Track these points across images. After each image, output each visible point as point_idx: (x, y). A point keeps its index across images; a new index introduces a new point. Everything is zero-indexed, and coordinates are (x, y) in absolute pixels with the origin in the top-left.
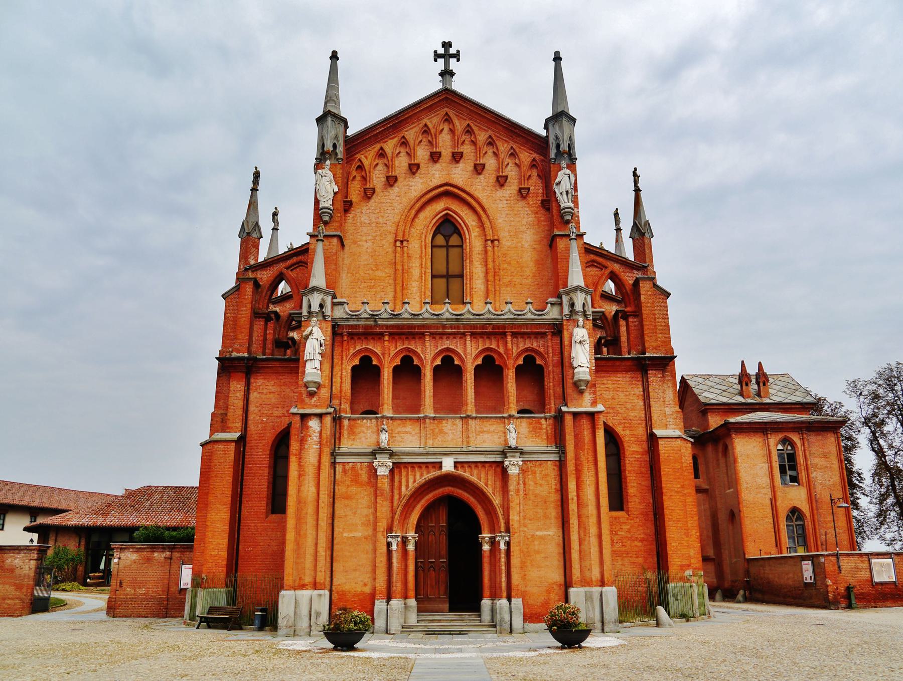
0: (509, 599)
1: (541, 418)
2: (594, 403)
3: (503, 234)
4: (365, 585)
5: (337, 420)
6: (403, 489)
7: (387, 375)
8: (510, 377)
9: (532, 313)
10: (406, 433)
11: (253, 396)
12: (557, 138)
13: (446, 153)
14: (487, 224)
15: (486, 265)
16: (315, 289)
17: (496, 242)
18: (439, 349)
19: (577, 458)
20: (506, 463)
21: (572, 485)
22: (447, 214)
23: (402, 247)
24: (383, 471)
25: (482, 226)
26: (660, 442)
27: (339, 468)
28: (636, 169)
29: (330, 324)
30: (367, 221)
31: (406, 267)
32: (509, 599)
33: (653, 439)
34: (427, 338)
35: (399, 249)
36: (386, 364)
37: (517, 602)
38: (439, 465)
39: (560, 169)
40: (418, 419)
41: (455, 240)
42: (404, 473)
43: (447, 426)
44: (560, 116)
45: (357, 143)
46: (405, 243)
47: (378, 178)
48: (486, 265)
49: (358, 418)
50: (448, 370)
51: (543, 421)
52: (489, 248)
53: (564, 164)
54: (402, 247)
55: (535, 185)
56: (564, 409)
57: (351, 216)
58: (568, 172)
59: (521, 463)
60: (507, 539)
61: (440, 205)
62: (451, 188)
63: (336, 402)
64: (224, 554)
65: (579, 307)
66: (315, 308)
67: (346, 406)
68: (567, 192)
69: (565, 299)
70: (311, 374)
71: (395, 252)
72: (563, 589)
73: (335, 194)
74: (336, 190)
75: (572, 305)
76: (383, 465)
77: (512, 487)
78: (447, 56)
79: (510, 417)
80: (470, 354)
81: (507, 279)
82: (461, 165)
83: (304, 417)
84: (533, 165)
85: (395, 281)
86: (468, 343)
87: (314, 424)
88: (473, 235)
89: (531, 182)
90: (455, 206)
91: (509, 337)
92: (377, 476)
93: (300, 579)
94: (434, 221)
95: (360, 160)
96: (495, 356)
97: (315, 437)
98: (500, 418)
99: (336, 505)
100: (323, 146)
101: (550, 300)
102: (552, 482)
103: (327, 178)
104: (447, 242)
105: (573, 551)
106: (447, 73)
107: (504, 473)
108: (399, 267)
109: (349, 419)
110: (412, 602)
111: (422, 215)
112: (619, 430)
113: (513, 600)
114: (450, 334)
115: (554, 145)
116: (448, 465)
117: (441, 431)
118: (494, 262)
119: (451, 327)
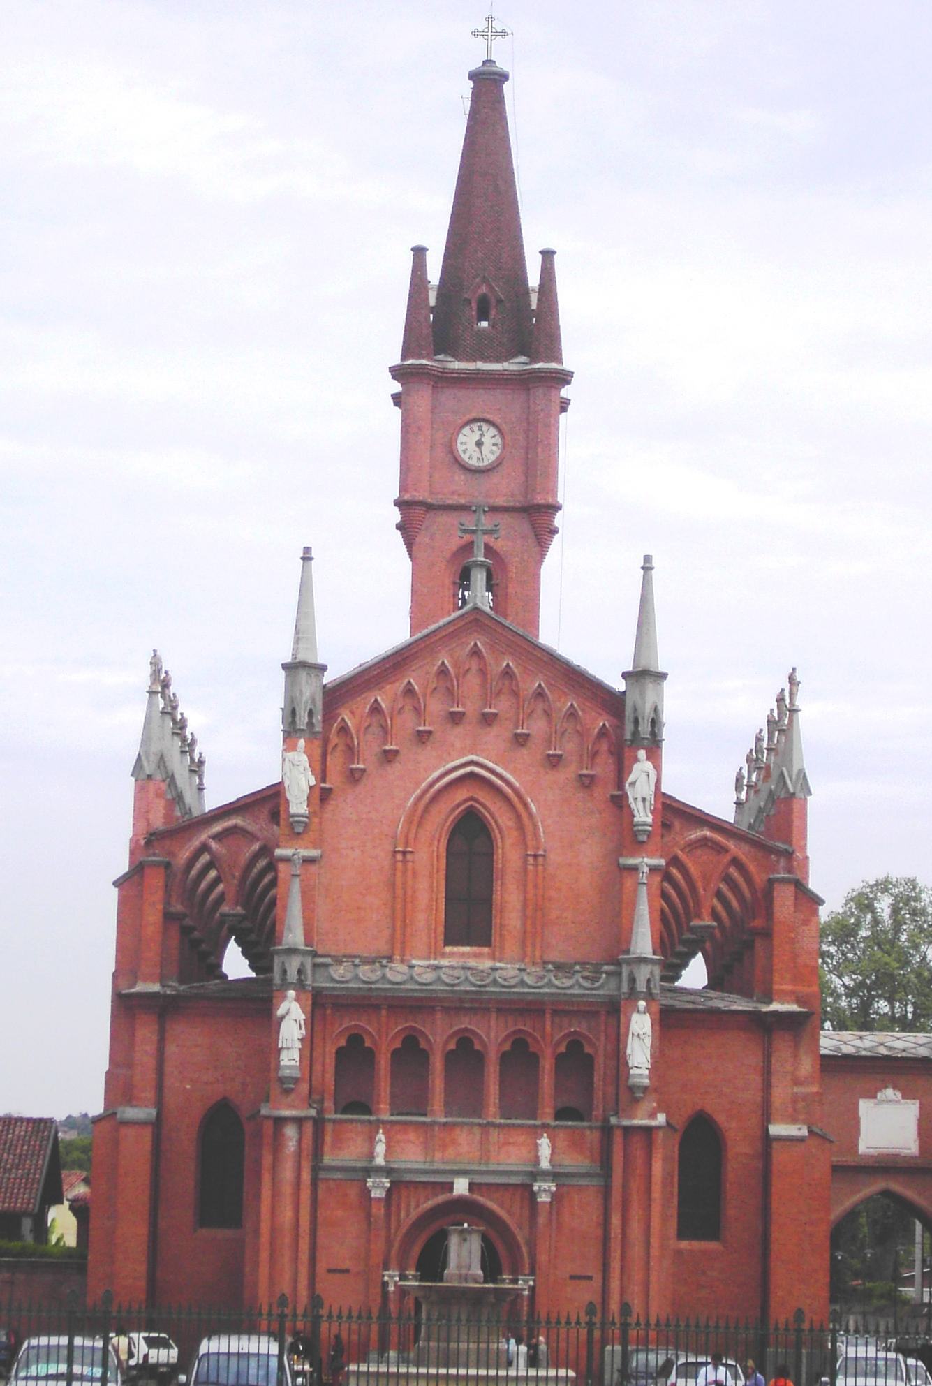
1: (584, 1128)
2: (653, 1116)
5: (319, 1123)
6: (403, 1214)
7: (383, 1063)
8: (547, 1064)
9: (581, 986)
10: (409, 1141)
11: (171, 1049)
12: (635, 710)
13: (470, 706)
15: (525, 892)
16: (292, 951)
17: (540, 859)
18: (456, 1028)
19: (625, 1186)
20: (536, 1188)
21: (616, 1220)
22: (471, 806)
23: (405, 862)
24: (377, 1193)
25: (521, 827)
26: (775, 1145)
27: (321, 1186)
28: (794, 669)
29: (310, 995)
30: (354, 817)
31: (410, 892)
33: (767, 1140)
34: (439, 1015)
35: (400, 865)
36: (384, 1048)
38: (450, 1187)
39: (636, 760)
40: (424, 1123)
42: (404, 1193)
43: (462, 1136)
45: (337, 695)
46: (409, 857)
47: (369, 747)
48: (525, 892)
49: (346, 1121)
50: (466, 1054)
51: (588, 1132)
52: (530, 867)
53: (642, 754)
54: (405, 862)
55: (603, 768)
56: (613, 1120)
57: (330, 808)
58: (648, 766)
59: (554, 1189)
61: (461, 795)
63: (316, 1097)
64: (142, 1284)
65: (641, 986)
66: (292, 976)
67: (329, 1104)
68: (644, 800)
69: (625, 971)
70: (289, 1067)
71: (394, 868)
73: (311, 788)
74: (313, 782)
75: (633, 980)
76: (378, 1188)
77: (542, 1220)
79: (545, 1127)
80: (493, 1035)
81: (553, 915)
82: (495, 730)
83: (280, 1122)
84: (603, 732)
86: (493, 1022)
87: (290, 1131)
88: (508, 842)
89: (598, 760)
90: (483, 796)
91: (548, 1016)
92: (370, 1199)
94: (451, 818)
95: (343, 719)
96: (529, 1040)
97: (291, 1146)
98: (530, 1126)
99: (320, 1233)
100: (293, 712)
101: (606, 968)
102: (595, 1215)
103: (301, 769)
105: (612, 1302)
107: (533, 1195)
108: (399, 892)
109: (334, 1121)
111: (434, 810)
112: (721, 1119)
114: (471, 1009)
115: (631, 719)
116: (461, 1186)
117: (454, 1142)
118: (536, 886)
119: (472, 1001)
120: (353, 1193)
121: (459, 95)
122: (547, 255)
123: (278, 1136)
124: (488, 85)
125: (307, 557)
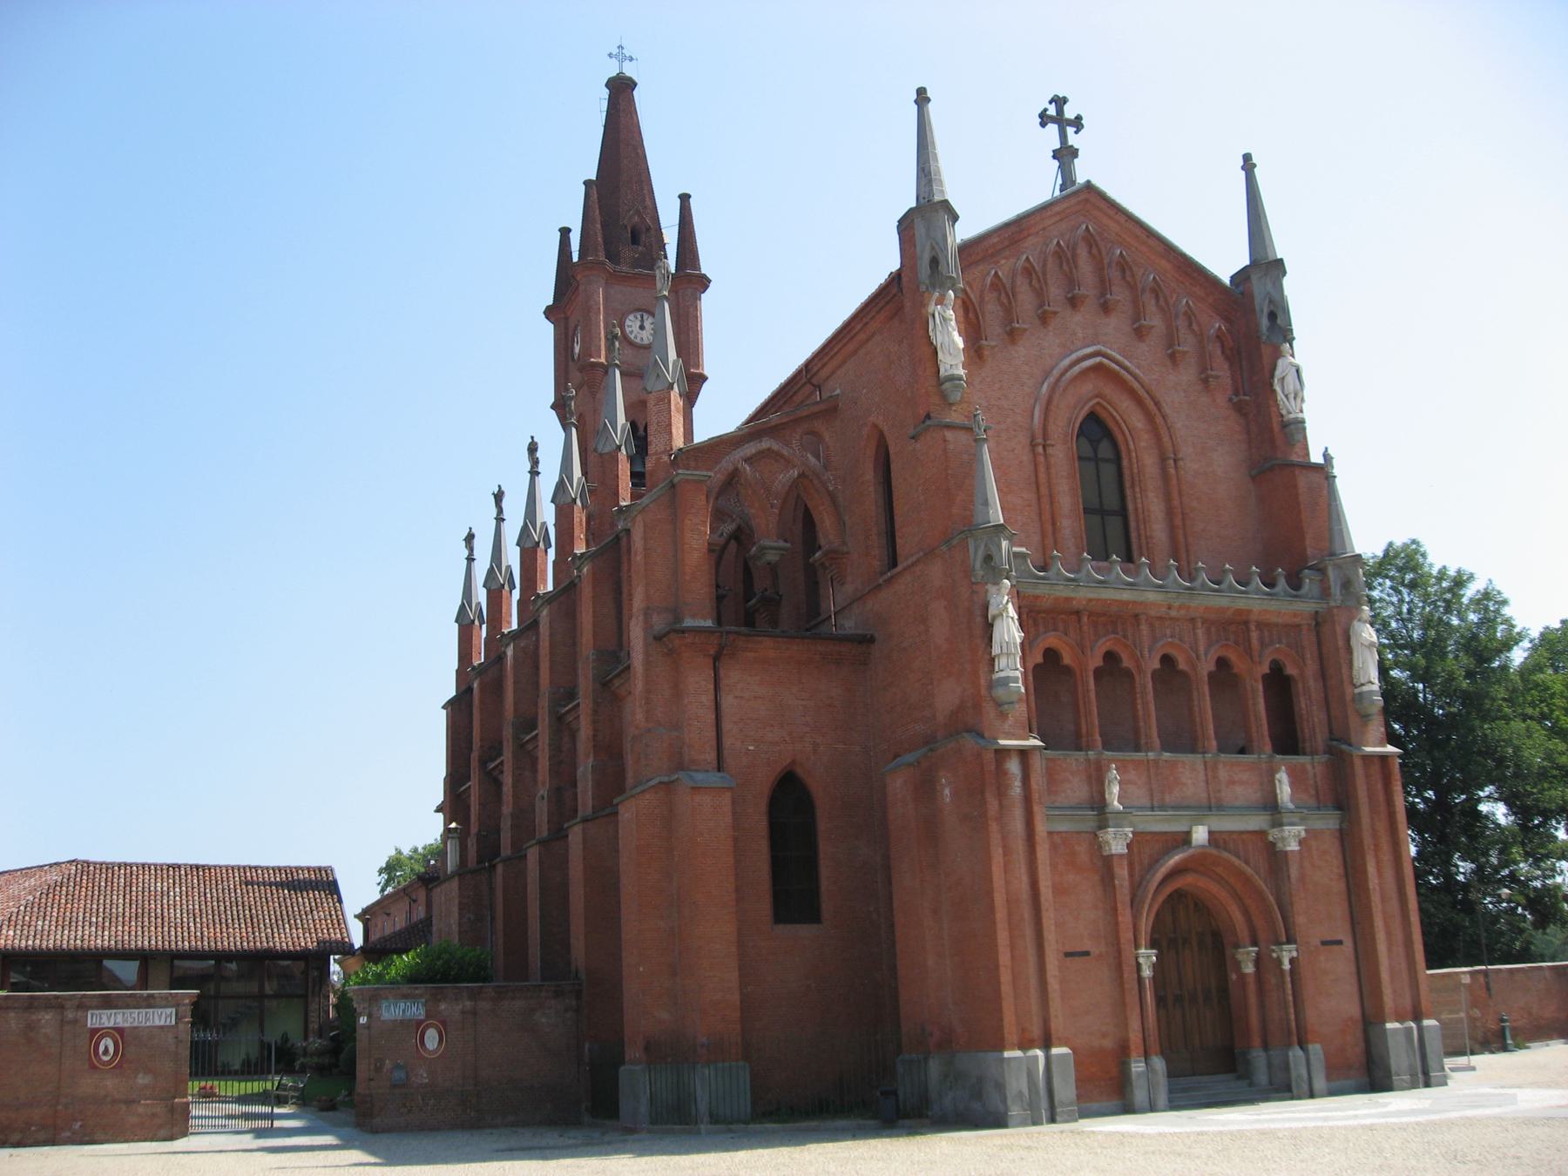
0: (1302, 1044)
3: (1186, 451)
4: (1104, 1035)
11: (728, 701)
14: (1164, 432)
32: (1302, 1044)
37: (1315, 1049)
38: (1185, 839)
41: (1105, 449)
44: (1265, 266)
59: (1303, 834)
60: (1295, 954)
61: (1087, 388)
62: (1105, 361)
72: (1360, 1026)
78: (1060, 120)
85: (1040, 514)
90: (1109, 390)
93: (1023, 1030)
104: (1095, 451)
106: (1065, 155)
108: (1044, 490)
110: (1159, 1063)
113: (1310, 1047)
120: (1082, 850)
121: (599, 99)
122: (685, 199)
123: (1001, 772)
124: (621, 90)
125: (922, 98)
